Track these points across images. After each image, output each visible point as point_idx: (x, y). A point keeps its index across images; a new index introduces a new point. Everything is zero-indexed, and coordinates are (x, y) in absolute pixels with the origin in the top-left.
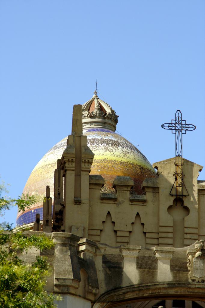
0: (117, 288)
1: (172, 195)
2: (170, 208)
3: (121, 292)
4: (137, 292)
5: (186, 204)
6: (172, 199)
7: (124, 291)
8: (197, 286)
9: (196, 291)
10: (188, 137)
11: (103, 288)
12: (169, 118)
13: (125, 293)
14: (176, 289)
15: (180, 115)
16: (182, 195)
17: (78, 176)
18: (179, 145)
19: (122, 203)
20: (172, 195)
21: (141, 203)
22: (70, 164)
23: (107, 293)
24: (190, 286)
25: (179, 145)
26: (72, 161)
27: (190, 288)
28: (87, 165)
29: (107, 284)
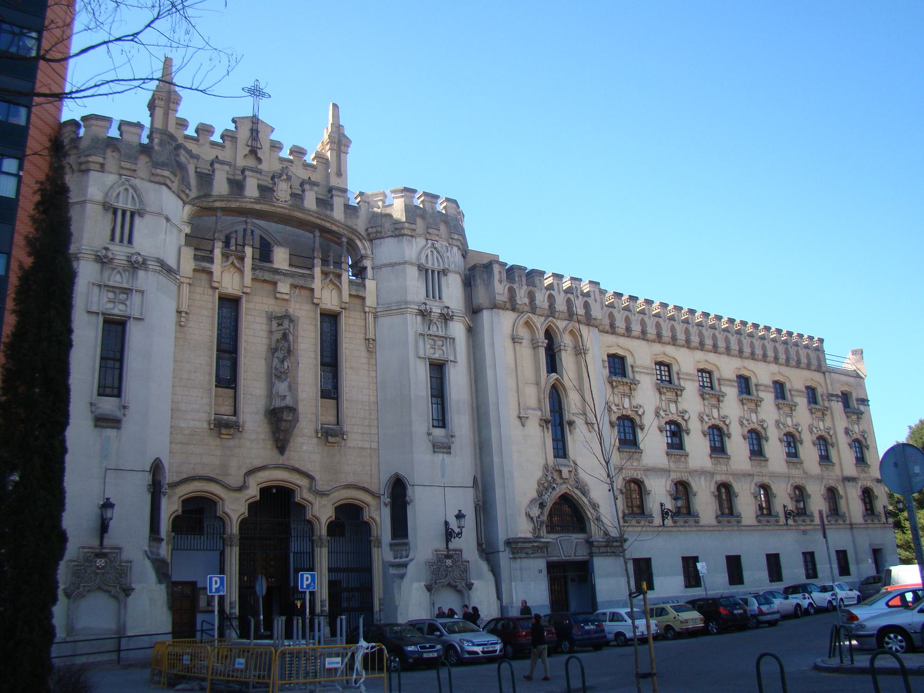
0: (208, 195)
1: (248, 146)
2: (245, 156)
3: (211, 200)
4: (226, 202)
5: (259, 155)
6: (249, 149)
7: (214, 199)
8: (280, 205)
9: (279, 209)
10: (263, 102)
11: (193, 194)
12: (250, 84)
13: (215, 201)
14: (261, 206)
15: (258, 84)
16: (257, 147)
17: (166, 114)
18: (256, 107)
19: (202, 145)
20: (248, 146)
21: (220, 148)
22: (160, 101)
23: (198, 198)
24: (274, 204)
25: (256, 107)
26: (162, 100)
27: (274, 206)
28: (175, 105)
29: (199, 190)
